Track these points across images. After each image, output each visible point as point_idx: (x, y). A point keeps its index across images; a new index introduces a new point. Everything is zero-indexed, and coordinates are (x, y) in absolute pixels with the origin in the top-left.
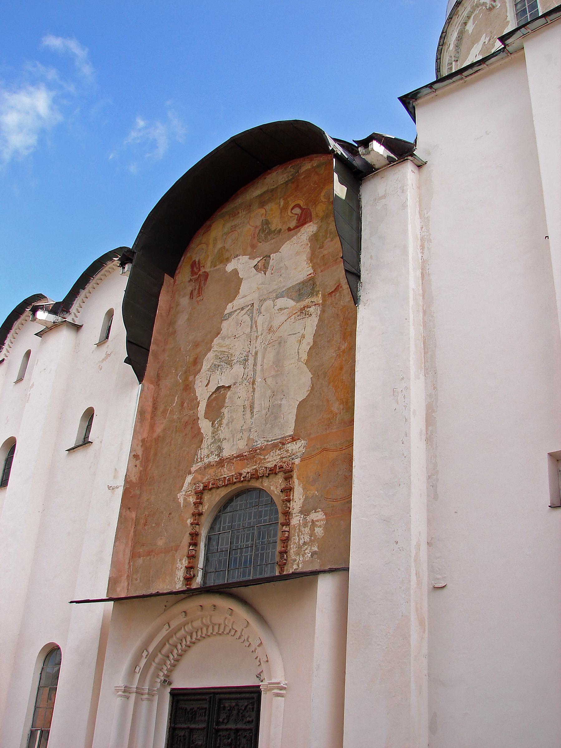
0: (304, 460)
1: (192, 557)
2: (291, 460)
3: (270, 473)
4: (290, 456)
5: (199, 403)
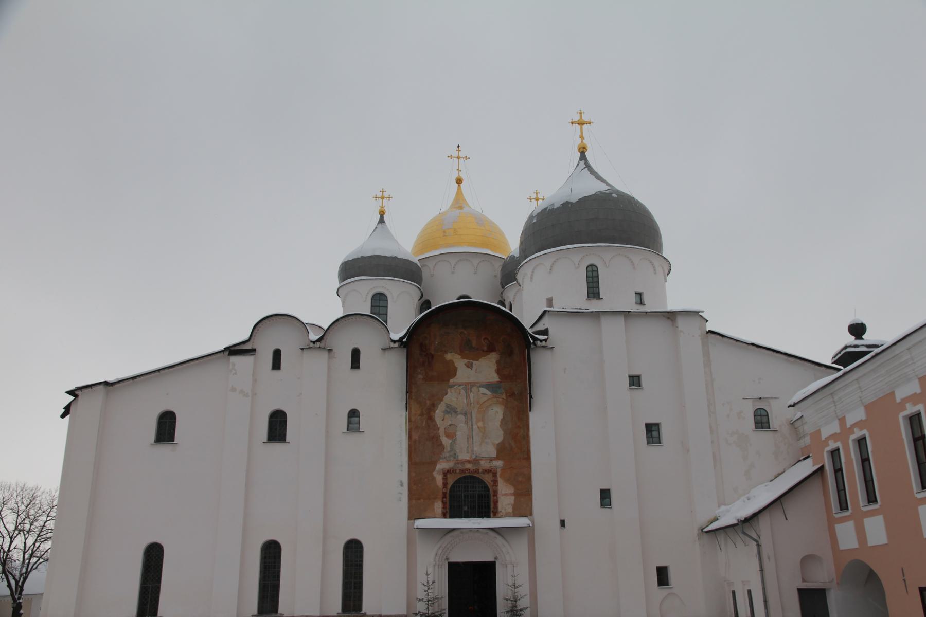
5: (439, 428)
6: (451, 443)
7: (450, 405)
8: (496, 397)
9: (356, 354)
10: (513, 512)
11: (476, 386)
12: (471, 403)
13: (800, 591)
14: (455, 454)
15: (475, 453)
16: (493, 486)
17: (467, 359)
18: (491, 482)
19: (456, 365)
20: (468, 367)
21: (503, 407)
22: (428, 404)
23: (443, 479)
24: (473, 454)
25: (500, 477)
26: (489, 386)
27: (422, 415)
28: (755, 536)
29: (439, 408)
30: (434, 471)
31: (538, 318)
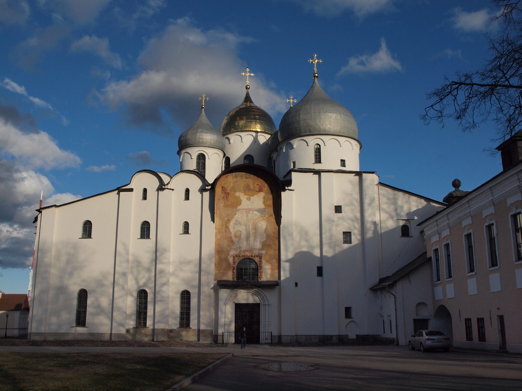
1: (233, 272)
6: (238, 241)
7: (238, 220)
8: (263, 216)
9: (187, 191)
10: (270, 277)
11: (252, 210)
12: (249, 220)
13: (415, 321)
14: (240, 247)
15: (250, 246)
16: (260, 264)
17: (247, 195)
19: (241, 198)
20: (248, 200)
21: (266, 222)
22: (226, 220)
23: (233, 259)
24: (250, 247)
26: (259, 211)
27: (222, 225)
28: (394, 293)
29: (231, 222)
30: (228, 255)
31: (286, 173)
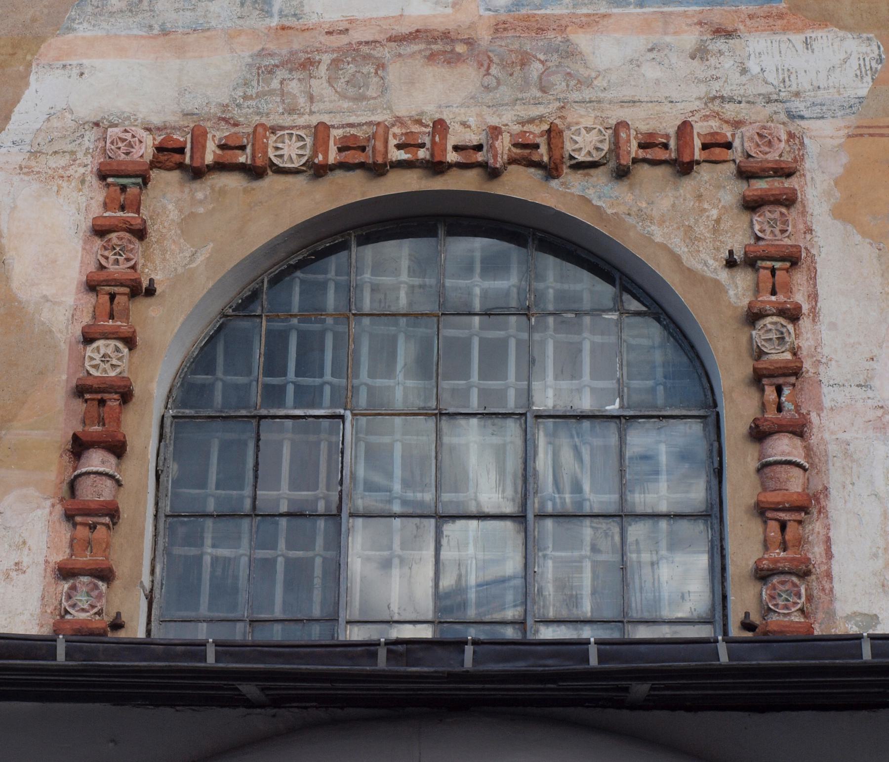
0: (871, 135)
2: (783, 117)
3: (645, 161)
4: (775, 97)
18: (724, 275)
23: (100, 231)
25: (838, 213)
